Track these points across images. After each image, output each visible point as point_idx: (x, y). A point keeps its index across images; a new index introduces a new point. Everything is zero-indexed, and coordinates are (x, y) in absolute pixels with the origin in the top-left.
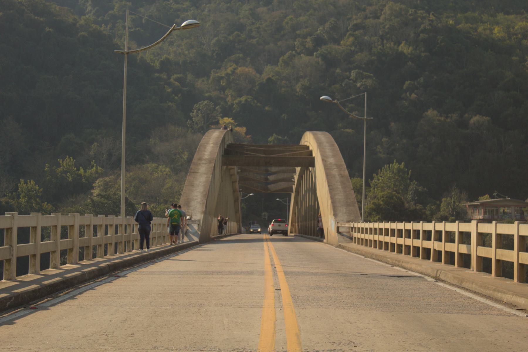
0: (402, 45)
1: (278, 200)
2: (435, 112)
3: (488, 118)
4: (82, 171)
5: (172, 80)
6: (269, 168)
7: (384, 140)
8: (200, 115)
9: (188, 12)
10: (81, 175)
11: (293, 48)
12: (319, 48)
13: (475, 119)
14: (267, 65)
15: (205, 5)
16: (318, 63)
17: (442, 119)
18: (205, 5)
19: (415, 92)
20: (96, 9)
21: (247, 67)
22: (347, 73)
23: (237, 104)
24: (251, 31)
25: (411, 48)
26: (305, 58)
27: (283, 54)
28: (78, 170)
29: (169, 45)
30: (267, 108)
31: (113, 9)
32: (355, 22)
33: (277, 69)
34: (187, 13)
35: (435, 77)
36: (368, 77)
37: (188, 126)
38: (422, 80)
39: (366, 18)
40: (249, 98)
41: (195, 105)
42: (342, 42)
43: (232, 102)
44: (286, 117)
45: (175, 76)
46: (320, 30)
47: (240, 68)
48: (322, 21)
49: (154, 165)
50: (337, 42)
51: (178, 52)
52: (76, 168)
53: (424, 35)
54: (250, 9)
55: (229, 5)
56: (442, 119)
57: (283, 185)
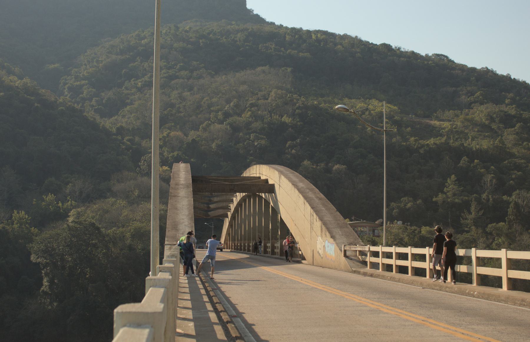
0: (285, 117)
1: (206, 224)
2: (309, 162)
3: (345, 166)
4: (60, 204)
5: (125, 140)
6: (212, 199)
8: (146, 164)
9: (135, 95)
10: (59, 207)
11: (209, 119)
12: (227, 119)
13: (336, 167)
15: (146, 91)
16: (227, 129)
17: (314, 167)
18: (146, 91)
19: (294, 148)
20: (71, 93)
21: (177, 132)
23: (171, 157)
24: (179, 108)
25: (290, 119)
26: (218, 126)
27: (202, 123)
28: (58, 203)
29: (122, 118)
31: (83, 94)
32: (251, 102)
33: (198, 133)
34: (134, 96)
35: (308, 139)
36: (262, 139)
37: (137, 172)
38: (298, 141)
39: (258, 99)
40: (179, 153)
41: (142, 157)
42: (243, 115)
43: (168, 156)
44: (205, 166)
45: (127, 138)
46: (227, 107)
48: (228, 101)
49: (113, 200)
50: (240, 115)
51: (128, 122)
52: (56, 202)
53: (299, 110)
54: (179, 93)
56: (314, 167)
57: (221, 212)
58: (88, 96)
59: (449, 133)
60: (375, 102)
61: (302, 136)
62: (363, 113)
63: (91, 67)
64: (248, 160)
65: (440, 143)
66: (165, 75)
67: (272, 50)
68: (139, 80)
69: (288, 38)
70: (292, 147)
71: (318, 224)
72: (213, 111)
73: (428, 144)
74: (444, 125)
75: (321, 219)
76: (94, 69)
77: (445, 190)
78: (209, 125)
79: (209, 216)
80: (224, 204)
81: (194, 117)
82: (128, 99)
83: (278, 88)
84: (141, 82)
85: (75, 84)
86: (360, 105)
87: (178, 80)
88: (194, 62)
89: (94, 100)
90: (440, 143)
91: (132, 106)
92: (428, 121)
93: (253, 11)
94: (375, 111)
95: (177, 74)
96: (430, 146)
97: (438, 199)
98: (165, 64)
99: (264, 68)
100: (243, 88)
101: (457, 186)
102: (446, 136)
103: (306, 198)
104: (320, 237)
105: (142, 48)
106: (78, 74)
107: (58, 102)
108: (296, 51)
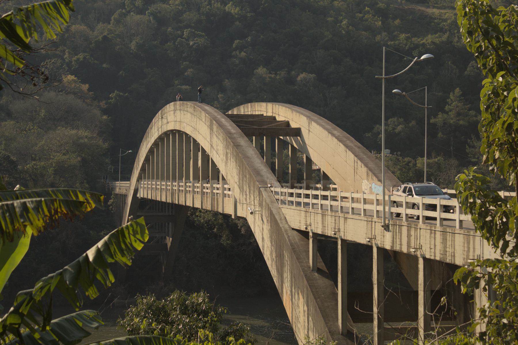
2: (265, 69)
3: (314, 75)
7: (220, 96)
12: (149, 8)
17: (273, 76)
22: (179, 32)
23: (75, 61)
25: (238, 9)
26: (138, 18)
30: (104, 66)
33: (109, 27)
36: (200, 36)
38: (249, 39)
40: (87, 56)
43: (70, 59)
44: (123, 74)
47: (74, 26)
56: (273, 76)
59: (453, 26)
61: (253, 32)
64: (182, 67)
65: (440, 42)
70: (241, 48)
73: (424, 43)
74: (446, 16)
77: (447, 108)
90: (440, 42)
92: (423, 9)
96: (427, 46)
97: (437, 120)
101: (462, 103)
102: (448, 33)
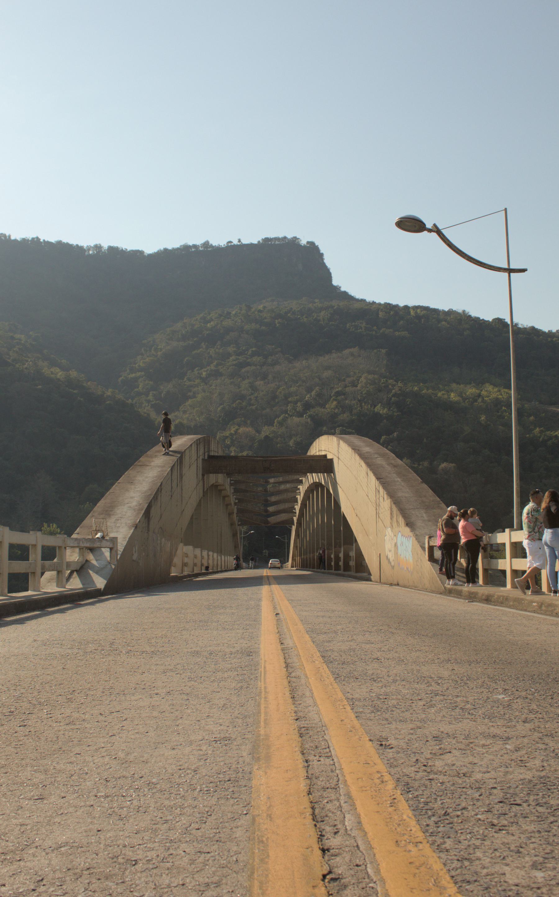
3: (454, 464)
6: (269, 498)
11: (286, 412)
13: (443, 465)
14: (264, 426)
16: (308, 423)
19: (391, 444)
24: (250, 399)
26: (296, 420)
27: (278, 416)
32: (337, 390)
33: (272, 429)
35: (407, 432)
39: (346, 387)
48: (309, 390)
50: (323, 406)
51: (190, 418)
54: (250, 383)
55: (232, 380)
57: (283, 517)
58: (144, 390)
60: (489, 387)
62: (476, 401)
63: (148, 357)
66: (234, 362)
67: (362, 329)
68: (204, 369)
69: (381, 314)
71: (386, 503)
72: (290, 402)
73: (556, 435)
75: (391, 495)
76: (152, 358)
78: (285, 419)
79: (268, 522)
80: (287, 506)
81: (268, 410)
82: (190, 391)
83: (369, 372)
84: (206, 371)
85: (130, 376)
86: (471, 391)
87: (250, 367)
88: (269, 346)
89: (151, 394)
91: (194, 399)
93: (340, 287)
94: (490, 398)
95: (249, 360)
98: (235, 349)
99: (352, 350)
100: (327, 374)
103: (370, 465)
104: (389, 529)
105: (207, 332)
106: (134, 366)
107: (105, 395)
108: (391, 330)
